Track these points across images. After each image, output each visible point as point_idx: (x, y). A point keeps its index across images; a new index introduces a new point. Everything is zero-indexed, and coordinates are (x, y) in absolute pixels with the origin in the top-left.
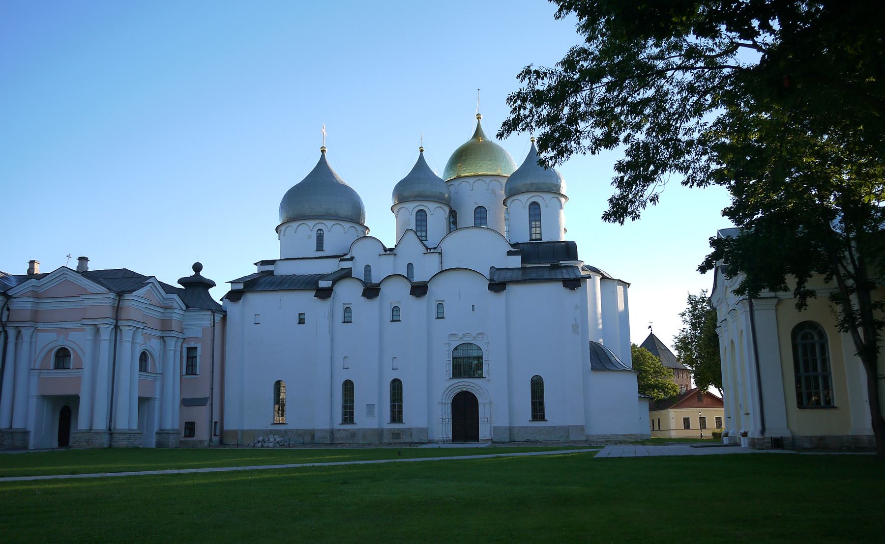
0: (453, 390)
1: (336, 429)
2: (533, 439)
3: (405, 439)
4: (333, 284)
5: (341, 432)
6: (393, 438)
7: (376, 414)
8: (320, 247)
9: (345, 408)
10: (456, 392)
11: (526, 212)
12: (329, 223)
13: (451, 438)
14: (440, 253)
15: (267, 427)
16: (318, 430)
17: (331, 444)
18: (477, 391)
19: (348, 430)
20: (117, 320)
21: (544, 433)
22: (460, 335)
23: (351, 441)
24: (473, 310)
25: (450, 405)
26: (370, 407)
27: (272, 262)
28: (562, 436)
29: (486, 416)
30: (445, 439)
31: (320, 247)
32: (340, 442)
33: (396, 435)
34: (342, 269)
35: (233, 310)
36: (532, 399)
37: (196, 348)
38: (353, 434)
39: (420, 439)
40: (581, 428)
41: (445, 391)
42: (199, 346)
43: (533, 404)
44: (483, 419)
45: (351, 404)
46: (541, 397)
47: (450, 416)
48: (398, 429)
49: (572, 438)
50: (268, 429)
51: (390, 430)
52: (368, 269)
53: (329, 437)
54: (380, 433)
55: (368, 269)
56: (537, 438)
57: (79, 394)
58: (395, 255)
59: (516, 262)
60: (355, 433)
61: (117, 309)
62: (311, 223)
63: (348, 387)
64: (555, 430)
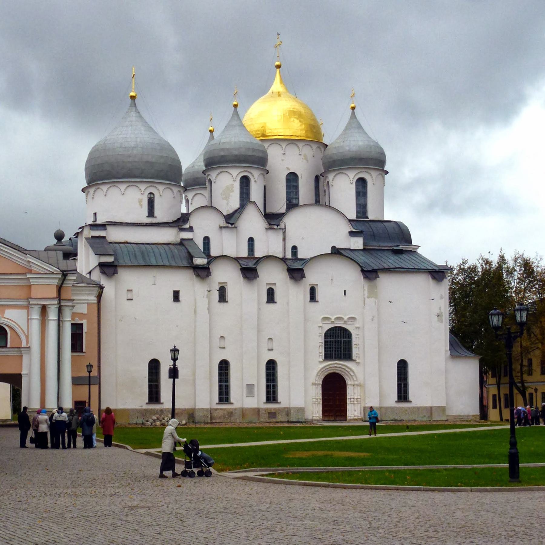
0: (325, 371)
1: (213, 409)
2: (399, 419)
3: (280, 418)
4: (209, 263)
5: (218, 411)
6: (269, 418)
7: (256, 394)
8: (151, 213)
9: (220, 387)
10: (326, 374)
11: (354, 186)
12: (161, 188)
13: (321, 418)
14: (284, 230)
15: (142, 406)
16: (199, 409)
17: (211, 423)
18: (346, 372)
19: (225, 409)
20: (60, 300)
21: (409, 413)
22: (333, 319)
23: (229, 421)
24: (345, 294)
25: (321, 386)
26: (250, 387)
27: (103, 226)
28: (425, 416)
29: (356, 397)
30: (318, 418)
31: (151, 213)
32: (218, 421)
33: (272, 414)
34: (182, 240)
35: (109, 286)
36: (398, 381)
37: (82, 324)
38: (231, 414)
39: (298, 418)
40: (443, 409)
41: (318, 373)
42: (84, 322)
43: (399, 386)
44: (352, 400)
45: (226, 384)
46: (404, 380)
47: (321, 398)
48: (275, 409)
49: (436, 417)
50: (143, 408)
51: (266, 410)
52: (207, 240)
53: (209, 416)
54: (257, 411)
55: (207, 240)
56: (402, 418)
57: (22, 373)
58: (236, 227)
59: (358, 243)
60: (232, 413)
61: (60, 289)
62: (143, 187)
63: (224, 366)
64: (419, 410)
